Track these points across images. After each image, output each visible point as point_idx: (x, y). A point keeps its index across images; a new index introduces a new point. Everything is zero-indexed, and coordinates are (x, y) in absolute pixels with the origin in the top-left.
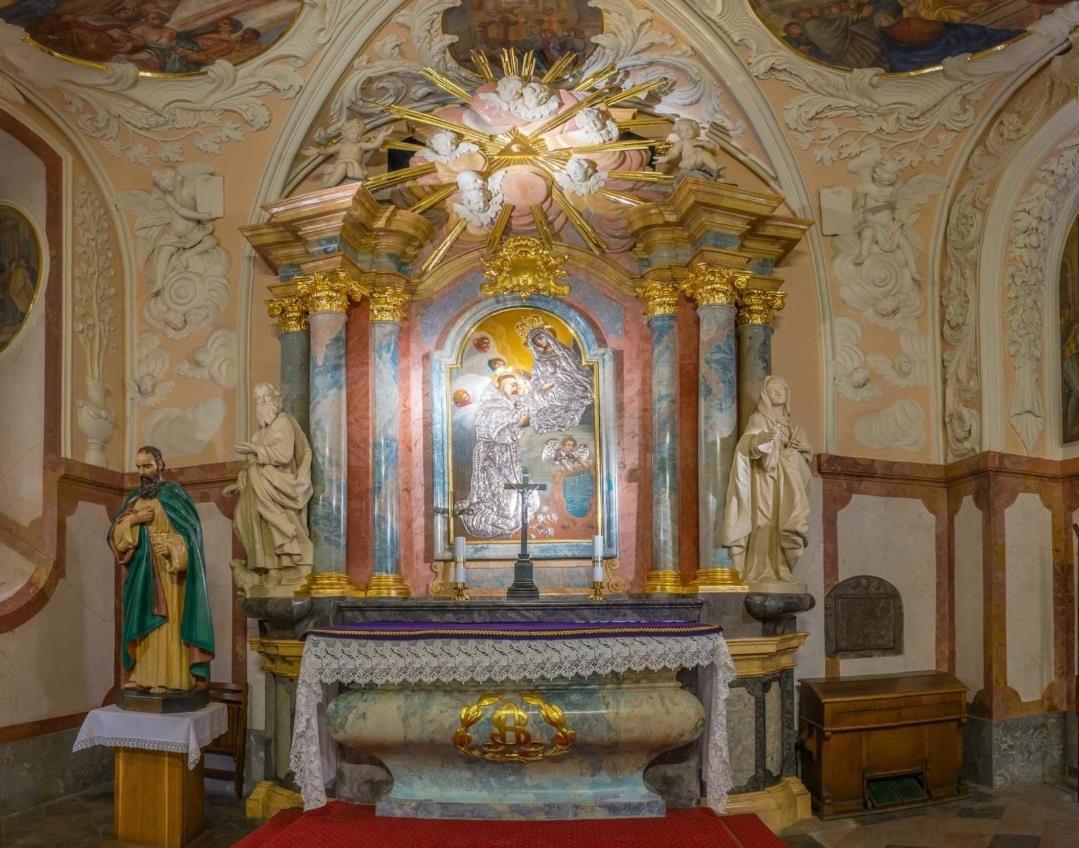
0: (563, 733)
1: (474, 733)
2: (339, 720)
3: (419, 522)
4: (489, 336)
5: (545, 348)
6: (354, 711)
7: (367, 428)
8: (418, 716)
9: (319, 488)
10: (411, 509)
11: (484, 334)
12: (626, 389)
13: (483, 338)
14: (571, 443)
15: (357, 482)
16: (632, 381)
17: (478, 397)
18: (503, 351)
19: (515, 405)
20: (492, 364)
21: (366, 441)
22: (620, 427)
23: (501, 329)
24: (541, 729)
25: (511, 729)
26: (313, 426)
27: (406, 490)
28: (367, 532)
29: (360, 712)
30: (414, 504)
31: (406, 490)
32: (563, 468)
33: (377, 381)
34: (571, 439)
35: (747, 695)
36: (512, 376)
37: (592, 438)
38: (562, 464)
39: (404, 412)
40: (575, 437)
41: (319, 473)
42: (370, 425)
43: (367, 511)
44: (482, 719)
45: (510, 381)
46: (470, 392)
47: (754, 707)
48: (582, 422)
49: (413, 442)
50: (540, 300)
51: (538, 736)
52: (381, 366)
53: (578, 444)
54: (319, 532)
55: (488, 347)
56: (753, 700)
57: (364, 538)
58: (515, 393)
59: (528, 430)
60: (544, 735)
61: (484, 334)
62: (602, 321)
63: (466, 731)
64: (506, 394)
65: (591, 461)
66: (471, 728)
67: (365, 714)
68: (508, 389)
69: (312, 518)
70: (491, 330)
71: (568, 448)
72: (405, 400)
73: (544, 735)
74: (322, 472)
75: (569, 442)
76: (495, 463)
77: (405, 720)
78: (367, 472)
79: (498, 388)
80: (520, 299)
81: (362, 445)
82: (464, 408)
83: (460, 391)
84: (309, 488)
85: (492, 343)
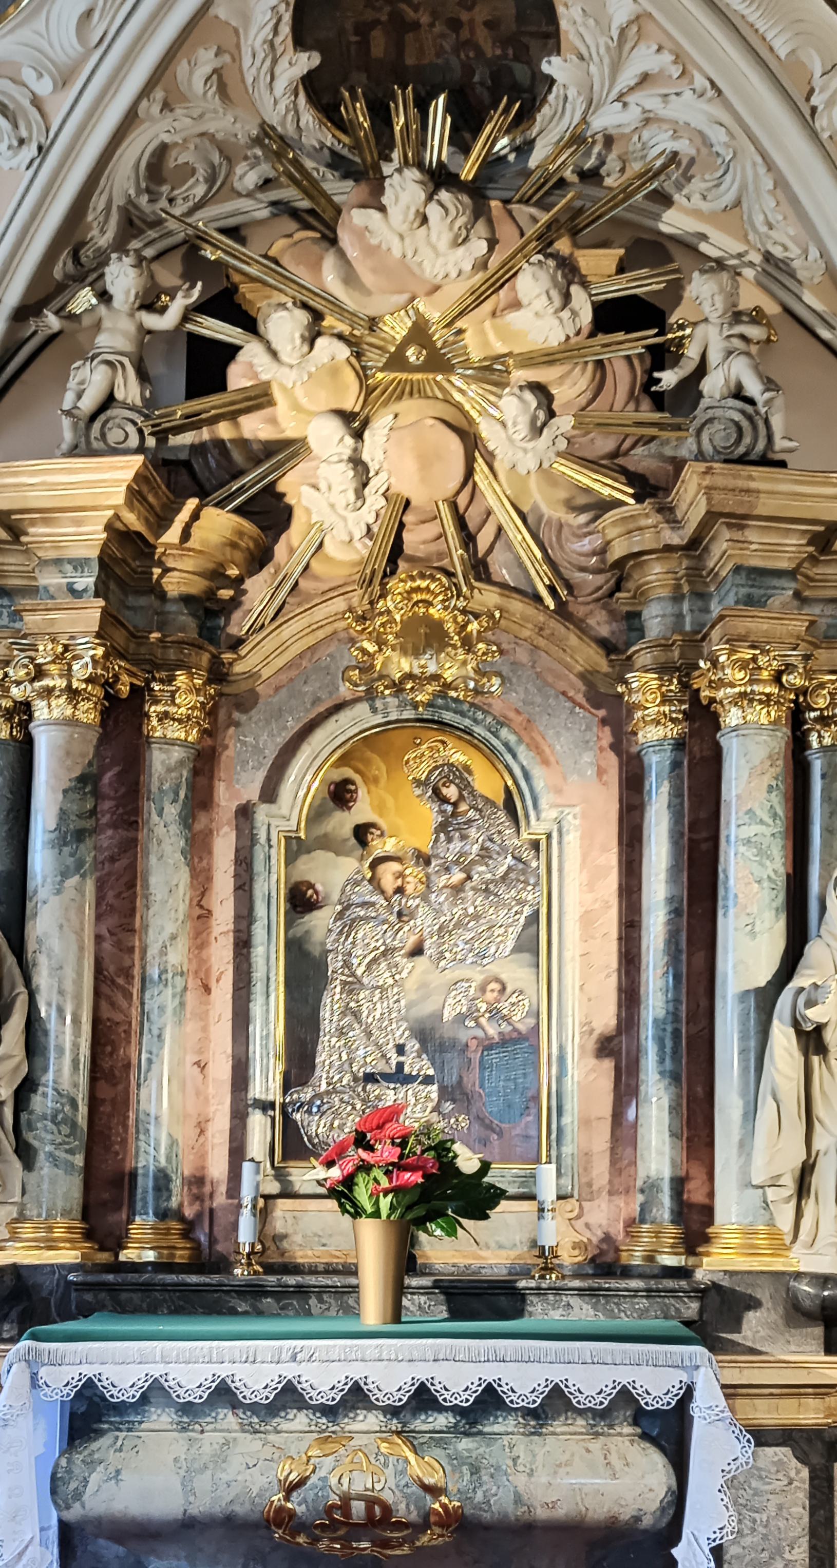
0: (443, 1506)
1: (299, 1504)
3: (221, 1123)
4: (357, 778)
5: (455, 805)
6: (100, 1468)
7: (131, 950)
8: (209, 1473)
9: (38, 1061)
10: (207, 1100)
11: (347, 772)
13: (347, 781)
14: (494, 986)
15: (109, 1049)
17: (335, 896)
18: (380, 808)
19: (400, 914)
20: (362, 833)
21: (127, 974)
23: (379, 767)
24: (406, 1496)
25: (360, 1498)
26: (31, 946)
27: (197, 1063)
28: (124, 1142)
30: (211, 1090)
31: (197, 1063)
32: (480, 1034)
33: (153, 860)
34: (497, 980)
37: (534, 977)
38: (478, 1025)
39: (199, 917)
40: (504, 977)
41: (39, 1033)
42: (137, 943)
43: (122, 1103)
44: (314, 1479)
45: (395, 866)
46: (319, 887)
48: (518, 949)
49: (214, 975)
50: (447, 709)
51: (403, 1511)
52: (160, 830)
53: (509, 990)
54: (35, 1143)
57: (117, 1153)
58: (400, 890)
59: (421, 962)
60: (412, 1508)
61: (347, 772)
63: (287, 1498)
64: (383, 892)
66: (295, 1494)
67: (118, 1472)
68: (389, 882)
69: (24, 1116)
70: (360, 766)
71: (490, 996)
72: (203, 894)
73: (412, 1508)
74: (46, 1033)
75: (494, 986)
76: (360, 1022)
77: (186, 1482)
78: (128, 1032)
79: (370, 881)
80: (415, 706)
81: (121, 981)
82: (307, 917)
83: (302, 883)
84: (17, 1068)
85: (362, 792)
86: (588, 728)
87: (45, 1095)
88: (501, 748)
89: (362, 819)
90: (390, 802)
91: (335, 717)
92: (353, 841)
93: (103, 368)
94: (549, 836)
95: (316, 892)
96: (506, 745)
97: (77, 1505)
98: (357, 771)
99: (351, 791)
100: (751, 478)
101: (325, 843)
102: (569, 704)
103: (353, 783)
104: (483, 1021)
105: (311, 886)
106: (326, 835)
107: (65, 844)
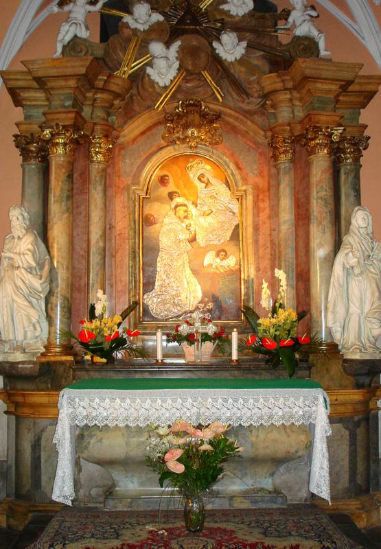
2: (84, 444)
6: (95, 438)
9: (54, 285)
12: (261, 214)
16: (264, 209)
18: (177, 186)
20: (171, 196)
22: (256, 242)
26: (50, 240)
29: (99, 438)
32: (218, 272)
34: (224, 251)
35: (343, 429)
36: (185, 205)
37: (238, 250)
45: (185, 208)
46: (155, 216)
47: (348, 437)
52: (96, 196)
55: (168, 182)
56: (347, 433)
61: (165, 172)
62: (243, 164)
64: (180, 218)
65: (238, 267)
67: (101, 439)
82: (151, 227)
86: (255, 156)
87: (57, 297)
88: (223, 163)
89: (170, 191)
90: (181, 183)
91: (161, 152)
92: (168, 198)
93: (74, 25)
94: (242, 196)
95: (154, 218)
96: (225, 162)
97: (86, 451)
98: (169, 171)
99: (166, 179)
100: (320, 65)
101: (158, 199)
102: (248, 147)
103: (168, 176)
104: (219, 267)
105: (152, 216)
106: (158, 196)
107: (63, 201)
